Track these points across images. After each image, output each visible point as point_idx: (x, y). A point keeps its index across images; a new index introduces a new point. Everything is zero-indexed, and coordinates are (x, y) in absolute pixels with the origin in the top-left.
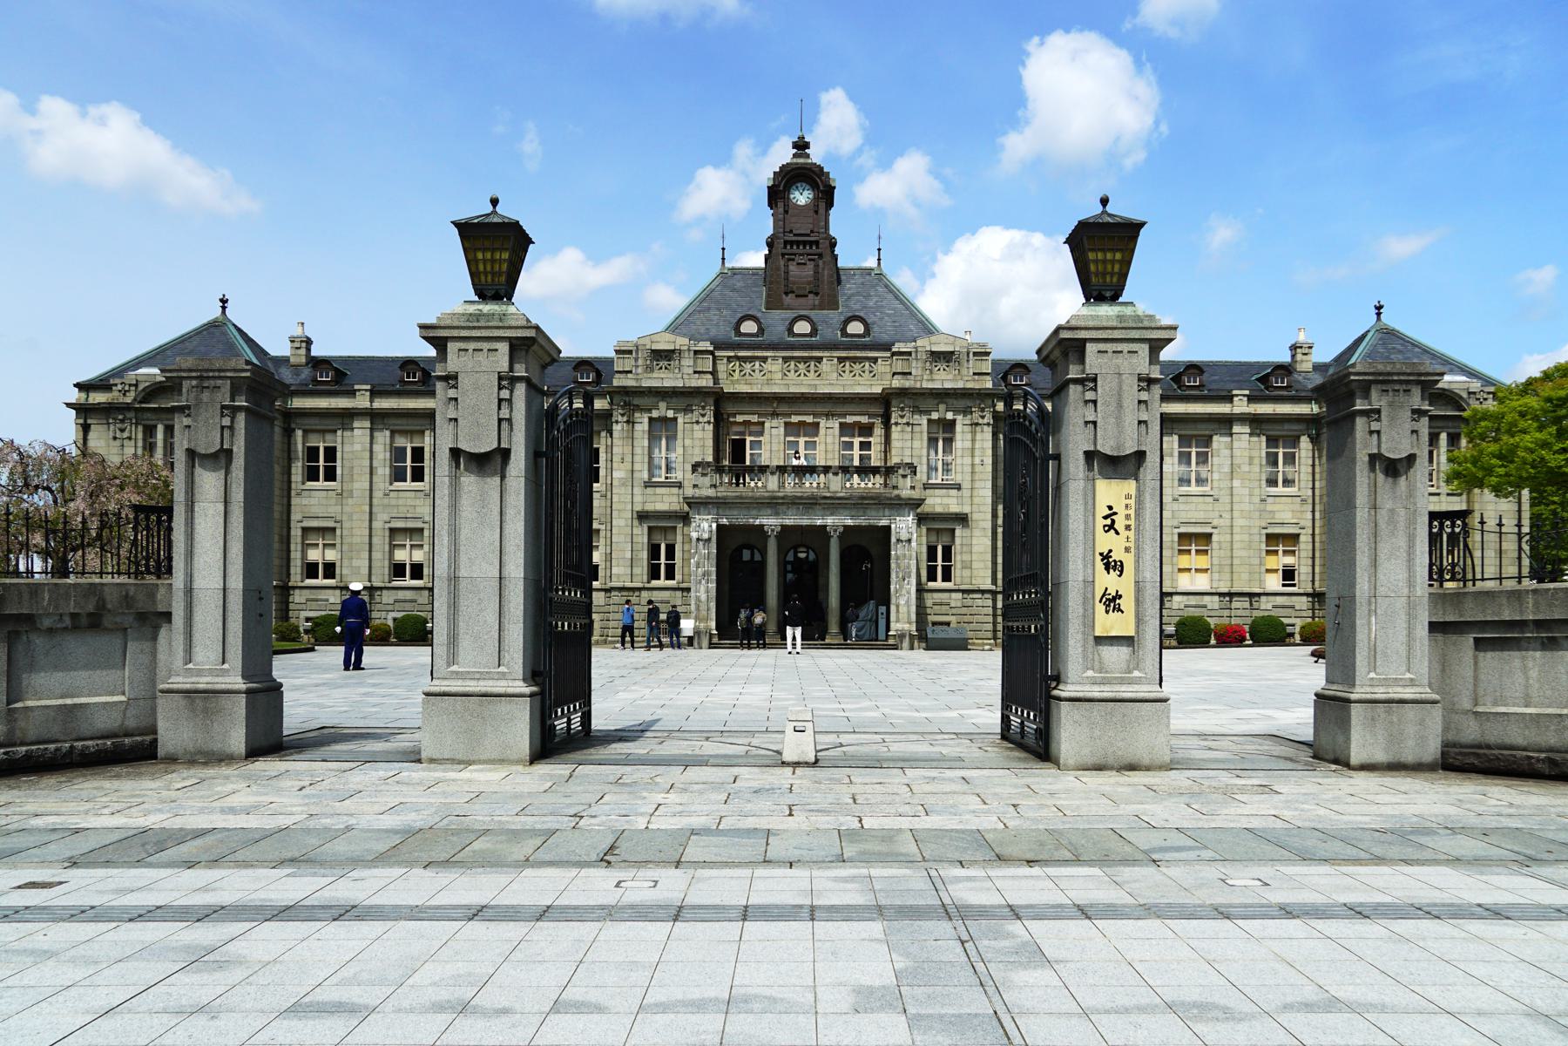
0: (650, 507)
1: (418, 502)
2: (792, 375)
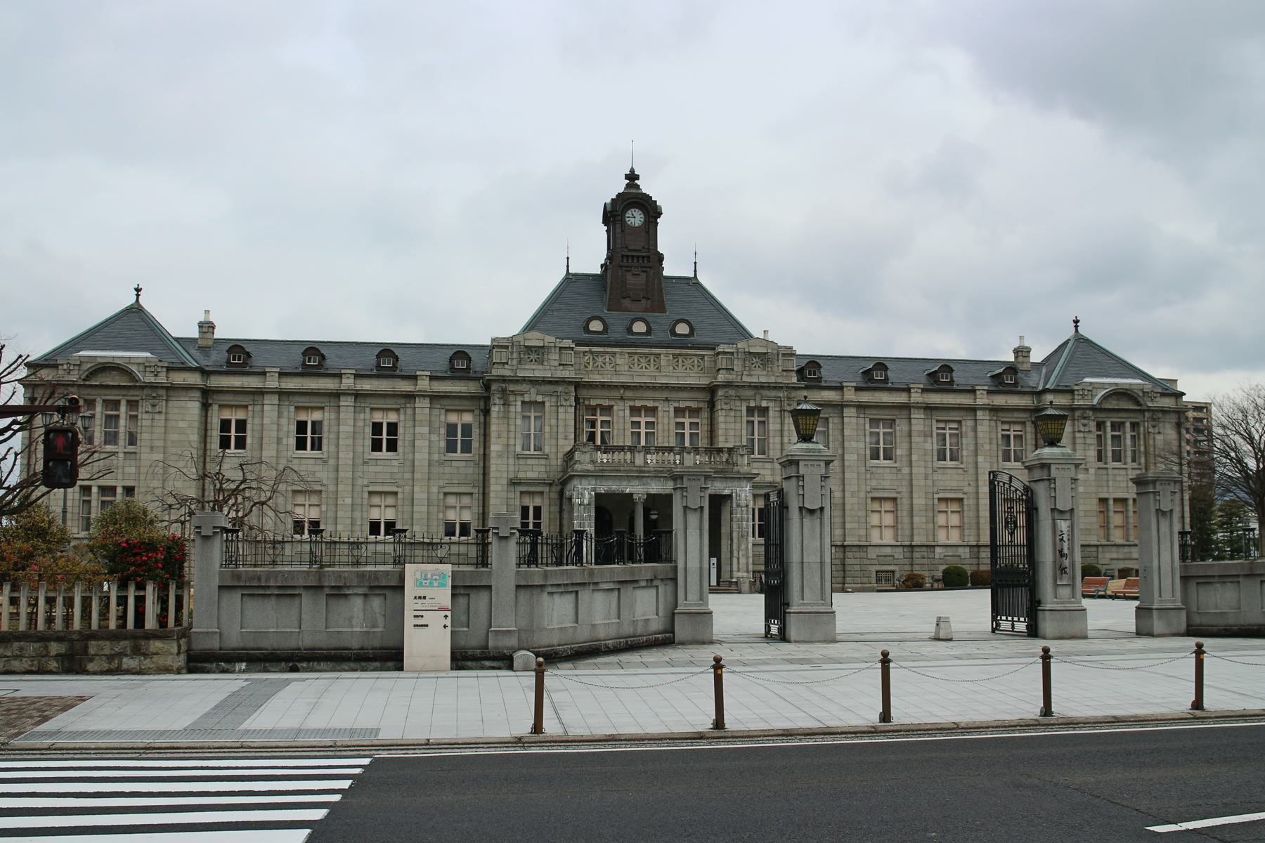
0: (521, 475)
1: (317, 468)
2: (636, 368)
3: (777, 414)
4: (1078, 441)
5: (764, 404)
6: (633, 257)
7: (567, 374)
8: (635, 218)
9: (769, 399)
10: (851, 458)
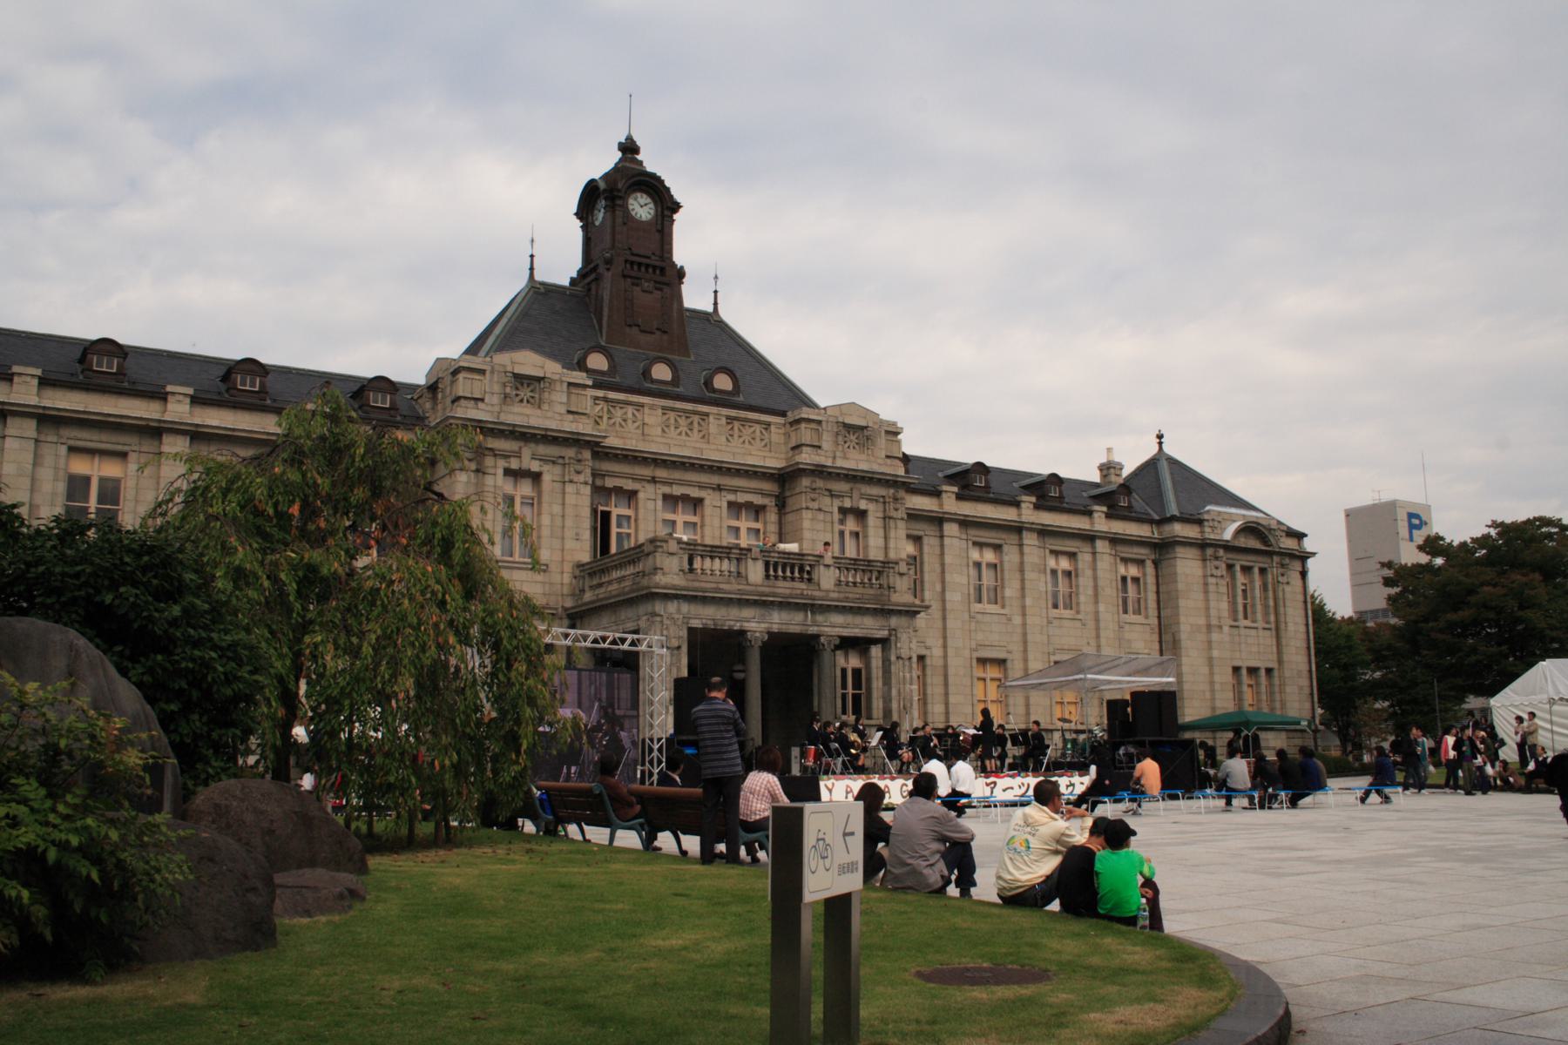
2: (672, 432)
3: (880, 523)
4: (1212, 588)
5: (863, 505)
6: (640, 264)
7: (584, 427)
8: (642, 208)
9: (871, 499)
10: (954, 597)
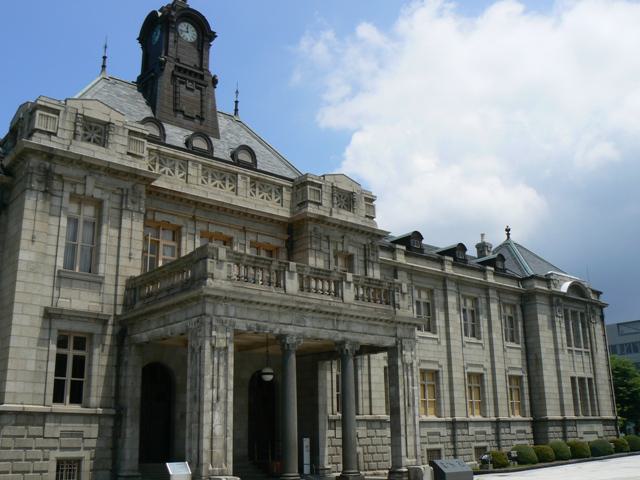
3: (362, 264)
5: (351, 250)
